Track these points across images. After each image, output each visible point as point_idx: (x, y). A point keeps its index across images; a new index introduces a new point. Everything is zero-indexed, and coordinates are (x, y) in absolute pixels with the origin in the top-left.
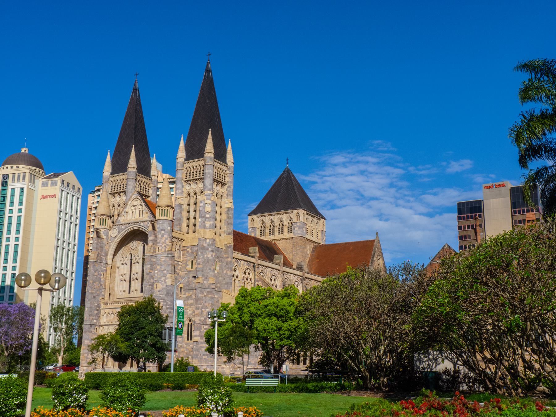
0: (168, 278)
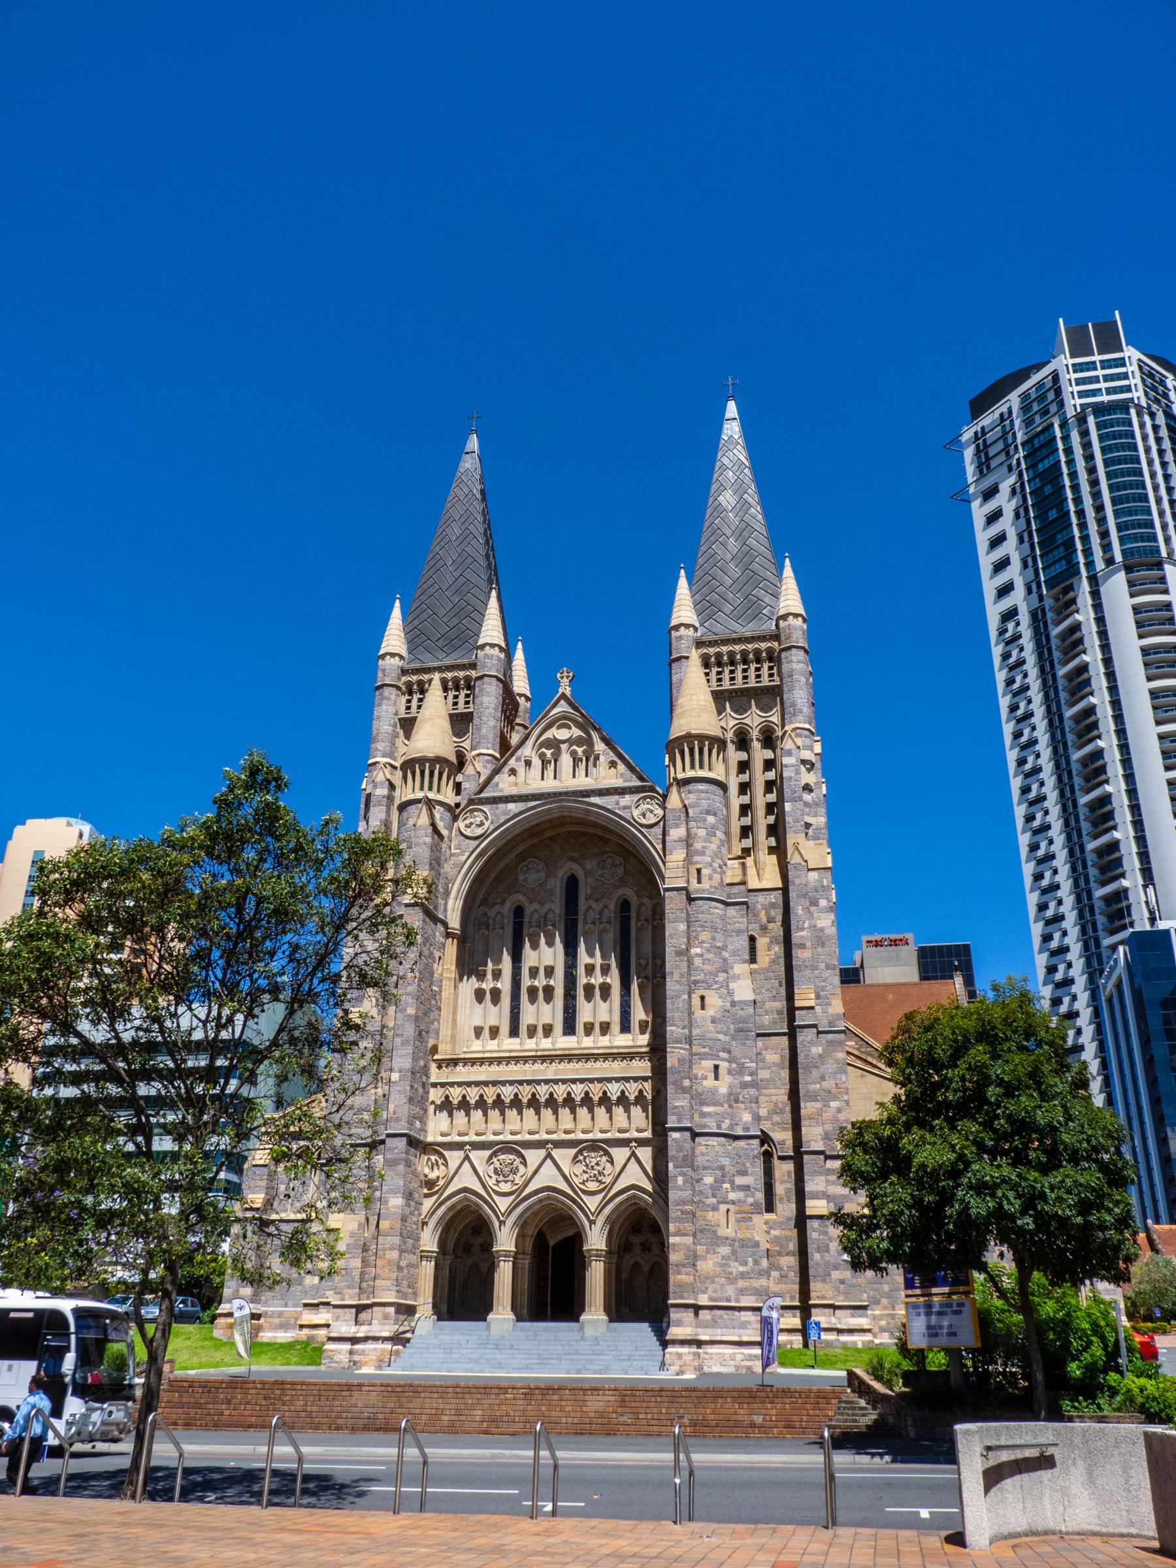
0: (737, 977)
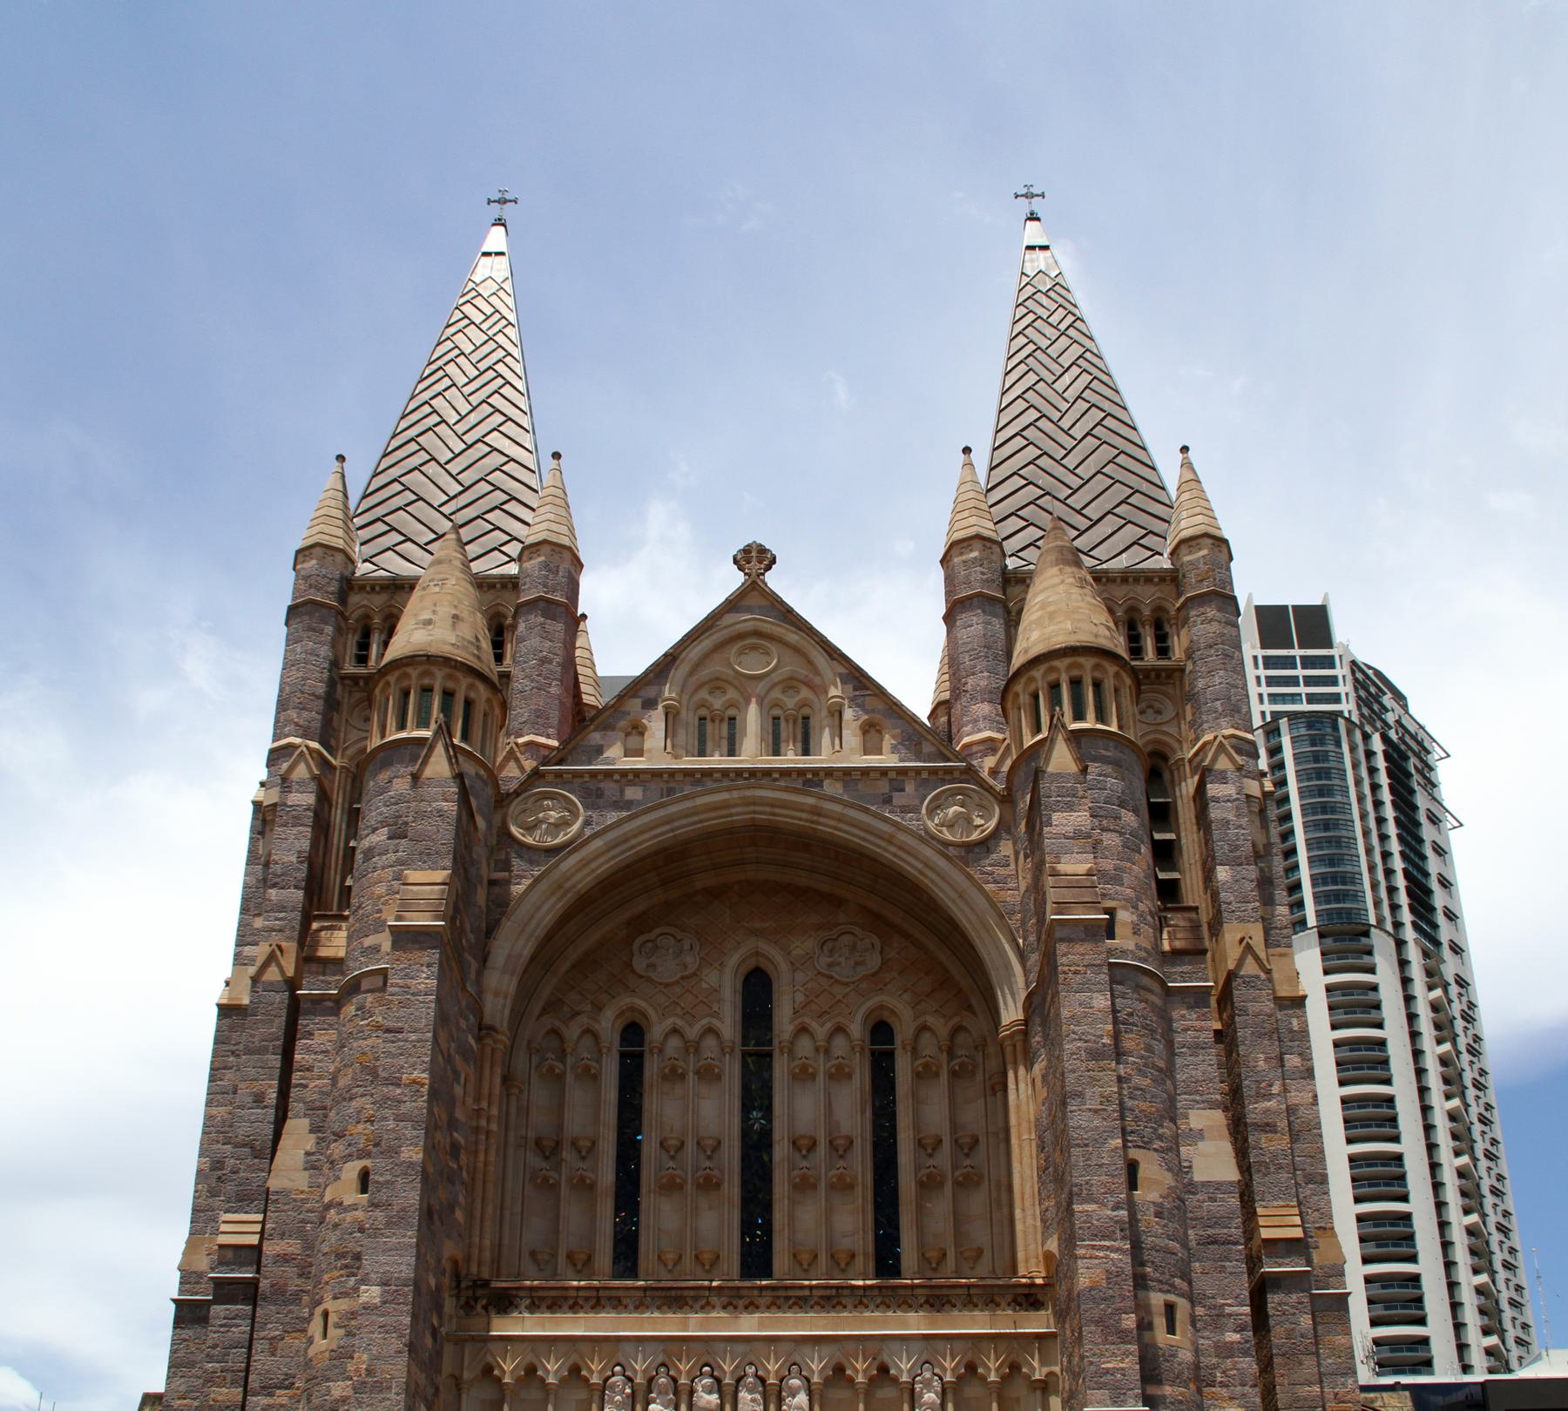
0: (1199, 1135)
